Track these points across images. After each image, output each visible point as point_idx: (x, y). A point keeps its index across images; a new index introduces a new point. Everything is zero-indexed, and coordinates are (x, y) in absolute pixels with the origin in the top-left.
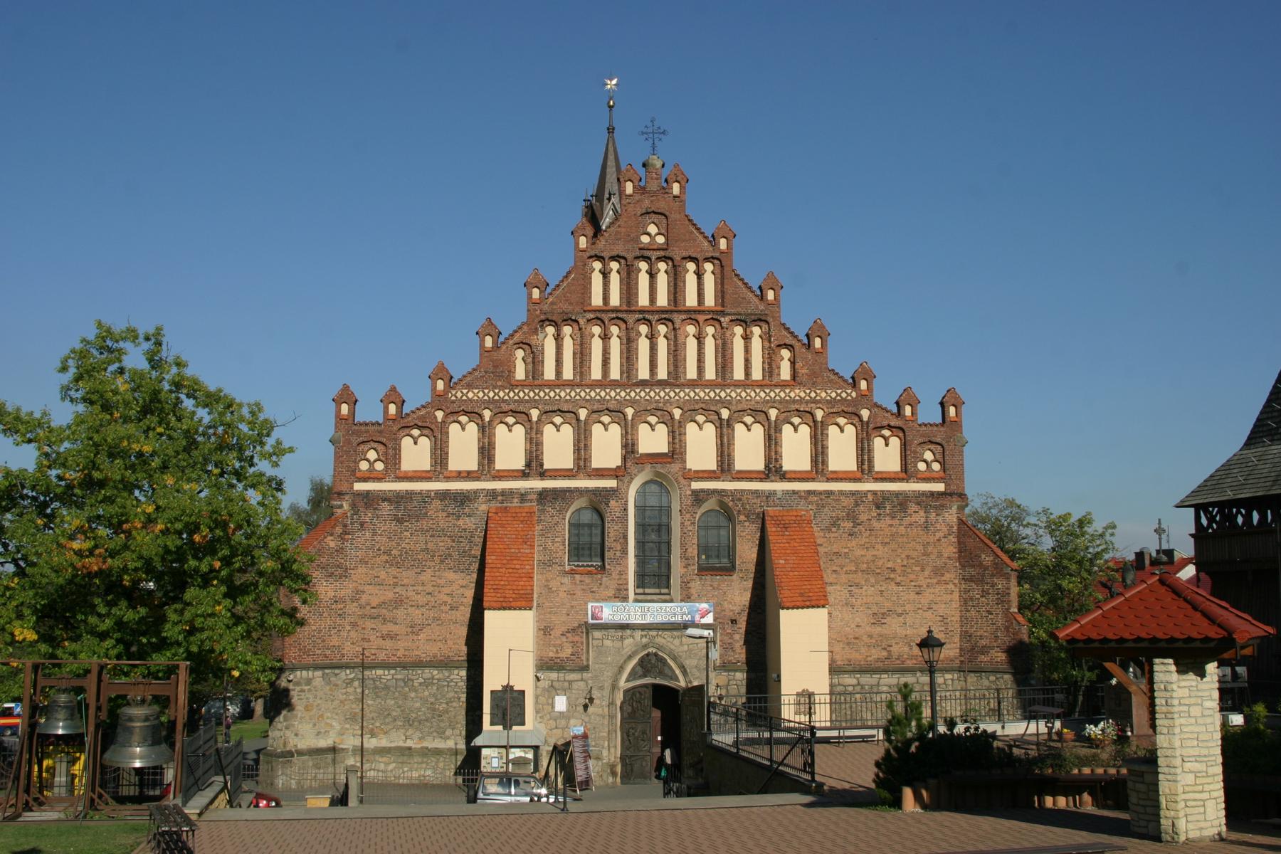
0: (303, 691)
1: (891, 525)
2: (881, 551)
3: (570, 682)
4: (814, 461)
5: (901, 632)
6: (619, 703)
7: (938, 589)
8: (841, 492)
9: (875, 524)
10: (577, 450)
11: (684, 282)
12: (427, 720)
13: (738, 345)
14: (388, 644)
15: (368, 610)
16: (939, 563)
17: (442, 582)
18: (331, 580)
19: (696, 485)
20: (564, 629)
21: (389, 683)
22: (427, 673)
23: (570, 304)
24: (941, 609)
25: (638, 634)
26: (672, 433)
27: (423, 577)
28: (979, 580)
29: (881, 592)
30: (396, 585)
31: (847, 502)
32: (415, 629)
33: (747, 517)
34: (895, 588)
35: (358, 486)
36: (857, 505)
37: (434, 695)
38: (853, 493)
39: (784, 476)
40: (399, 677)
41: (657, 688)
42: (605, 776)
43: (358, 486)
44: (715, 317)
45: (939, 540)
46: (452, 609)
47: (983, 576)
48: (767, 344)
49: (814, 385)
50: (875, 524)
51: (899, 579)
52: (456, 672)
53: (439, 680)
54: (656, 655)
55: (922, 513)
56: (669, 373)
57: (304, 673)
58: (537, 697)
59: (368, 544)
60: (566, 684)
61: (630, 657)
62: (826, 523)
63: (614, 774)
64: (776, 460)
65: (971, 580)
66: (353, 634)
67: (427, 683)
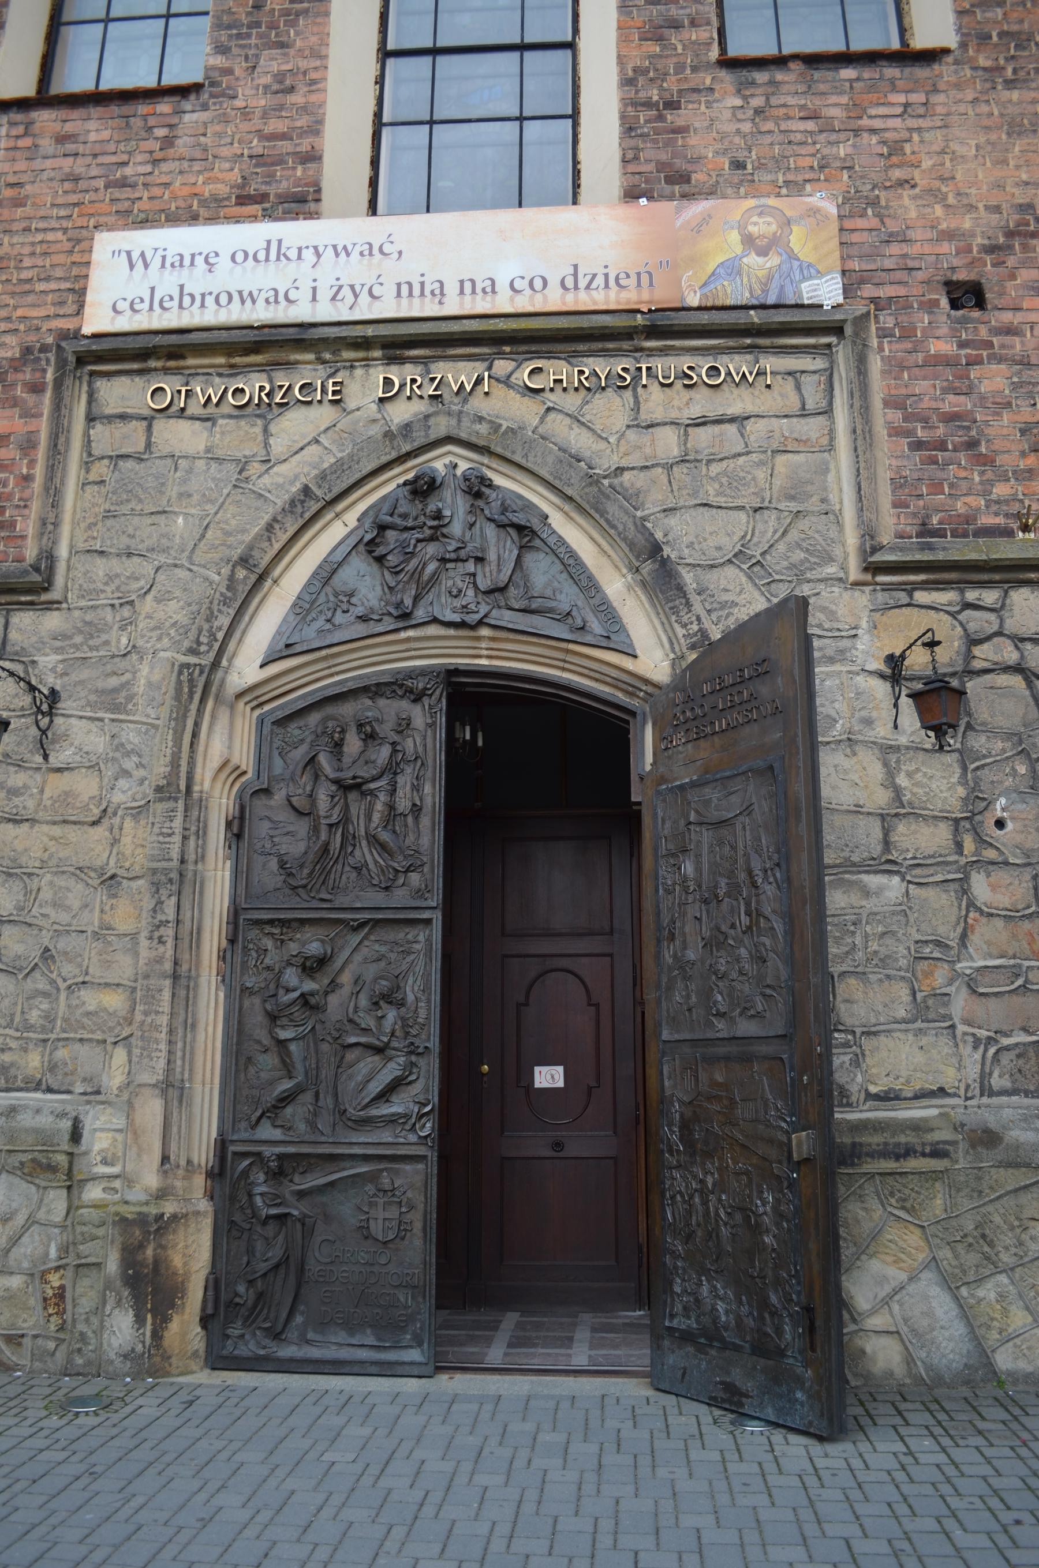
6: (221, 804)
25: (366, 384)
41: (467, 696)
42: (85, 1295)
54: (477, 489)
61: (310, 507)
63: (149, 1288)
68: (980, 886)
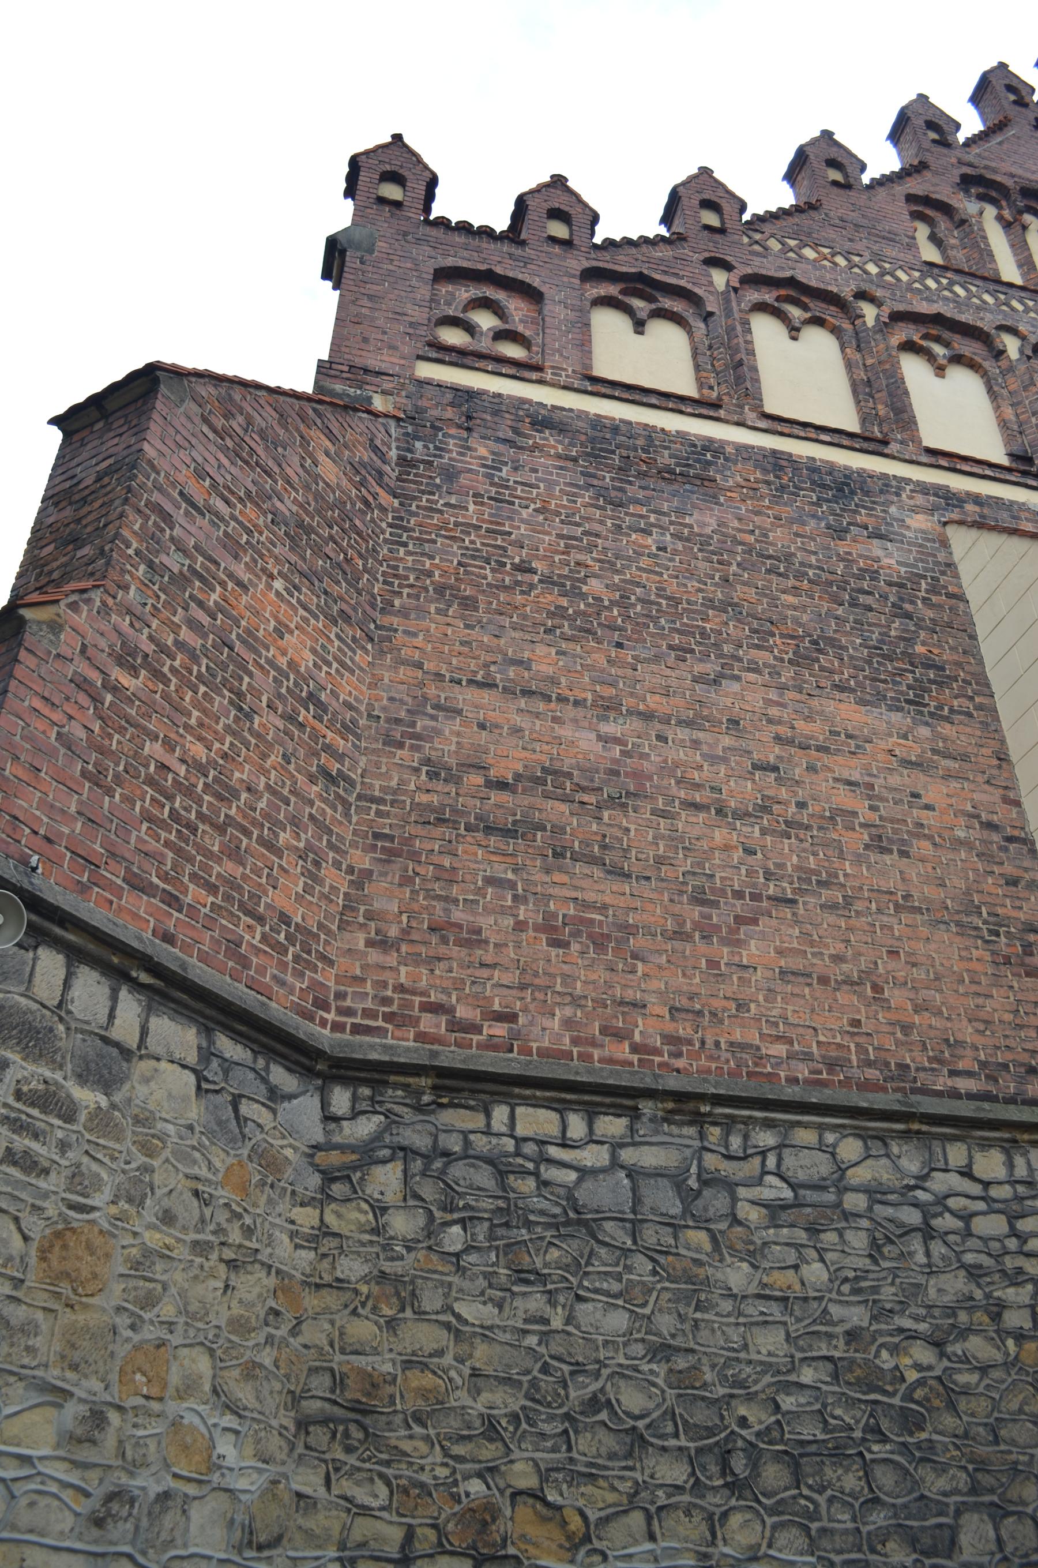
0: (48, 1100)
12: (837, 1454)
14: (584, 970)
17: (815, 730)
21: (599, 1195)
22: (806, 1153)
27: (728, 697)
30: (608, 708)
32: (713, 912)
37: (858, 1287)
40: (649, 1157)
46: (879, 844)
52: (957, 1154)
53: (875, 1193)
57: (90, 991)
66: (386, 897)
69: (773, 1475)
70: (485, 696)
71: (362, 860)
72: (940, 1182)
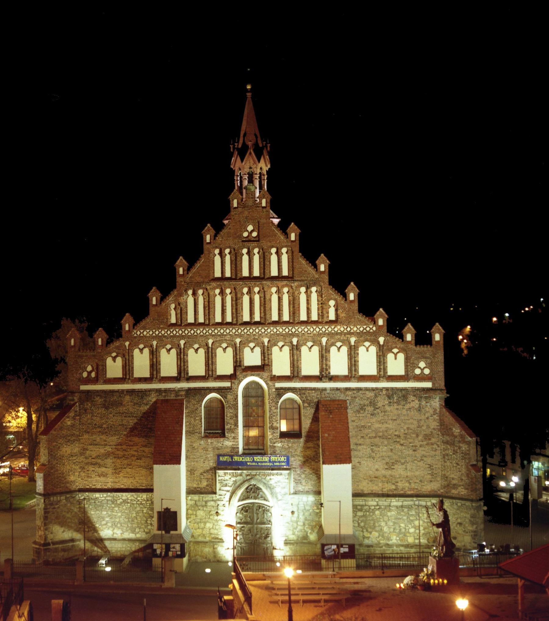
1: (397, 409)
2: (391, 425)
3: (206, 502)
4: (350, 370)
5: (403, 473)
7: (427, 447)
8: (367, 389)
9: (388, 408)
10: (207, 364)
11: (270, 262)
13: (303, 298)
14: (102, 479)
15: (90, 460)
16: (428, 432)
18: (69, 444)
19: (278, 385)
20: (201, 471)
23: (202, 277)
24: (429, 460)
26: (263, 353)
28: (452, 444)
29: (392, 450)
30: (106, 445)
31: (371, 394)
33: (309, 404)
34: (400, 447)
35: (83, 387)
36: (376, 396)
38: (373, 389)
39: (332, 378)
40: (108, 498)
43: (83, 387)
44: (290, 278)
45: (428, 418)
46: (137, 459)
47: (454, 441)
48: (320, 299)
49: (348, 324)
50: (388, 408)
51: (402, 442)
53: (131, 500)
55: (417, 402)
56: (261, 317)
58: (187, 510)
59: (89, 421)
60: (204, 503)
62: (357, 408)
64: (327, 370)
65: (447, 443)
67: (125, 502)
68: (299, 523)
69: (119, 525)
70: (91, 447)
71: (80, 470)
72: (139, 499)
